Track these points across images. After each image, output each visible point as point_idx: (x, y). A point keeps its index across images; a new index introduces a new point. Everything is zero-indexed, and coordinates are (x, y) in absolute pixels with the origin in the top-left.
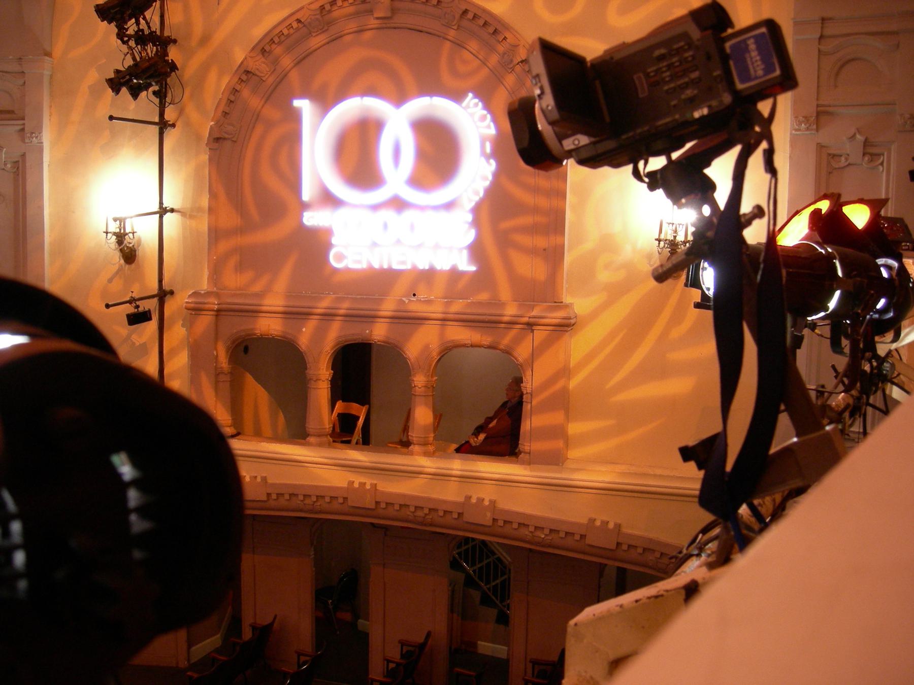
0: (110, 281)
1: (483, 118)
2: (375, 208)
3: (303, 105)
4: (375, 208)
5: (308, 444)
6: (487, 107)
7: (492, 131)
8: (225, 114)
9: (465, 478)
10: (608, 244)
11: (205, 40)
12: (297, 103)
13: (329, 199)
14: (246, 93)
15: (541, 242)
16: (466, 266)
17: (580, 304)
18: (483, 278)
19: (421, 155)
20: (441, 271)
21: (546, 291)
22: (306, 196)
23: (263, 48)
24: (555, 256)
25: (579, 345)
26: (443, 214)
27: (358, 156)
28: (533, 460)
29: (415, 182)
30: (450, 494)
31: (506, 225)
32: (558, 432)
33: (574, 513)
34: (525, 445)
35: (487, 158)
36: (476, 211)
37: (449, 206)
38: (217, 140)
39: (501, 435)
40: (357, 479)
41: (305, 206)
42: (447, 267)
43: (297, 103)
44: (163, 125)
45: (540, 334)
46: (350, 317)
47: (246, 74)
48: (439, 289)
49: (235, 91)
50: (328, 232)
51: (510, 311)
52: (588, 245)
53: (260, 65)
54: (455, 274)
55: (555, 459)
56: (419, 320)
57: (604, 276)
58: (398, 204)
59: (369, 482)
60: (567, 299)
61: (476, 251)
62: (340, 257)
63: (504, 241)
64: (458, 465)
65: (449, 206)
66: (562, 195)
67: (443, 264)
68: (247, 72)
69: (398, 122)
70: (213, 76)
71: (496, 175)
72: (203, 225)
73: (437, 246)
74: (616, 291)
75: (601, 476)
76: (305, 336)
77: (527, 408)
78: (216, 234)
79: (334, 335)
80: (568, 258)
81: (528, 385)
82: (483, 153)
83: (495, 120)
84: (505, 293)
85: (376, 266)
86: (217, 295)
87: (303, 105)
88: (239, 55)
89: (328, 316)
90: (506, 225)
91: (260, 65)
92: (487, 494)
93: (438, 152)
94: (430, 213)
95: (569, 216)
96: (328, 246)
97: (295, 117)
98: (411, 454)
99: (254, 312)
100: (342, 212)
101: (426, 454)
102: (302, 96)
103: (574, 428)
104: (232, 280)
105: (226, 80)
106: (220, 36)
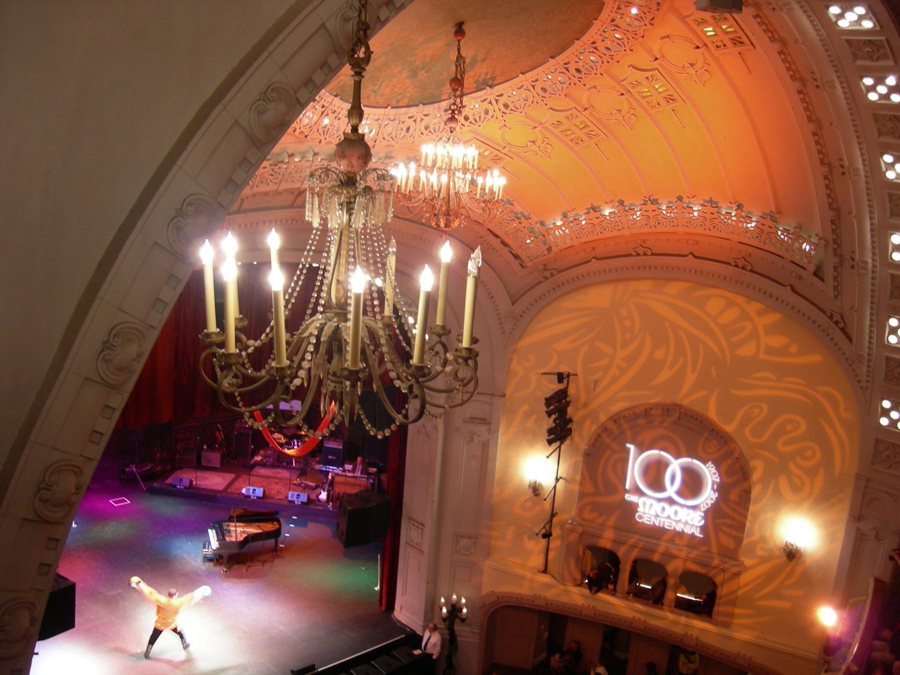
0: (525, 501)
1: (715, 474)
2: (660, 500)
3: (632, 447)
4: (660, 500)
5: (617, 597)
6: (717, 469)
7: (718, 480)
8: (593, 445)
9: (686, 625)
10: (763, 540)
11: (585, 405)
12: (628, 445)
13: (638, 492)
14: (604, 436)
15: (734, 533)
16: (698, 534)
17: (748, 562)
18: (705, 541)
19: (684, 482)
20: (687, 534)
21: (731, 554)
22: (627, 487)
23: (616, 419)
24: (739, 541)
25: (744, 578)
26: (691, 511)
27: (654, 476)
28: (716, 624)
29: (680, 493)
30: (679, 630)
31: (718, 521)
32: (732, 615)
33: (732, 648)
34: (714, 616)
35: (714, 491)
36: (706, 512)
37: (694, 508)
38: (587, 455)
39: (704, 608)
40: (637, 616)
41: (627, 491)
42: (690, 533)
43: (628, 445)
45: (727, 575)
46: (643, 549)
47: (604, 429)
48: (685, 541)
49: (599, 435)
50: (637, 505)
51: (716, 562)
52: (754, 538)
53: (612, 426)
54: (693, 536)
55: (727, 625)
56: (675, 557)
57: (759, 552)
58: (671, 501)
59: (642, 618)
60: (742, 559)
61: (703, 529)
62: (640, 517)
63: (717, 528)
64: (683, 619)
65: (694, 508)
66: (746, 517)
67: (688, 530)
68: (606, 429)
69: (675, 466)
70: (588, 423)
71: (717, 499)
72: (576, 487)
73: (686, 523)
74: (763, 560)
75: (744, 635)
76: (621, 552)
77: (717, 601)
78: (582, 495)
79: (634, 554)
80: (745, 542)
81: (721, 592)
82: (713, 488)
83: (720, 475)
84: (715, 549)
85: (657, 524)
86: (582, 526)
87: (632, 447)
88: (603, 418)
89: (634, 546)
90: (718, 521)
91: (612, 426)
92: (695, 633)
93: (692, 484)
94: (686, 510)
95: (748, 524)
96: (637, 511)
97: (627, 451)
98: (661, 609)
99: (600, 537)
100: (643, 499)
101: (671, 612)
102: (631, 443)
103: (737, 611)
104: (587, 515)
105: (594, 428)
106: (594, 404)
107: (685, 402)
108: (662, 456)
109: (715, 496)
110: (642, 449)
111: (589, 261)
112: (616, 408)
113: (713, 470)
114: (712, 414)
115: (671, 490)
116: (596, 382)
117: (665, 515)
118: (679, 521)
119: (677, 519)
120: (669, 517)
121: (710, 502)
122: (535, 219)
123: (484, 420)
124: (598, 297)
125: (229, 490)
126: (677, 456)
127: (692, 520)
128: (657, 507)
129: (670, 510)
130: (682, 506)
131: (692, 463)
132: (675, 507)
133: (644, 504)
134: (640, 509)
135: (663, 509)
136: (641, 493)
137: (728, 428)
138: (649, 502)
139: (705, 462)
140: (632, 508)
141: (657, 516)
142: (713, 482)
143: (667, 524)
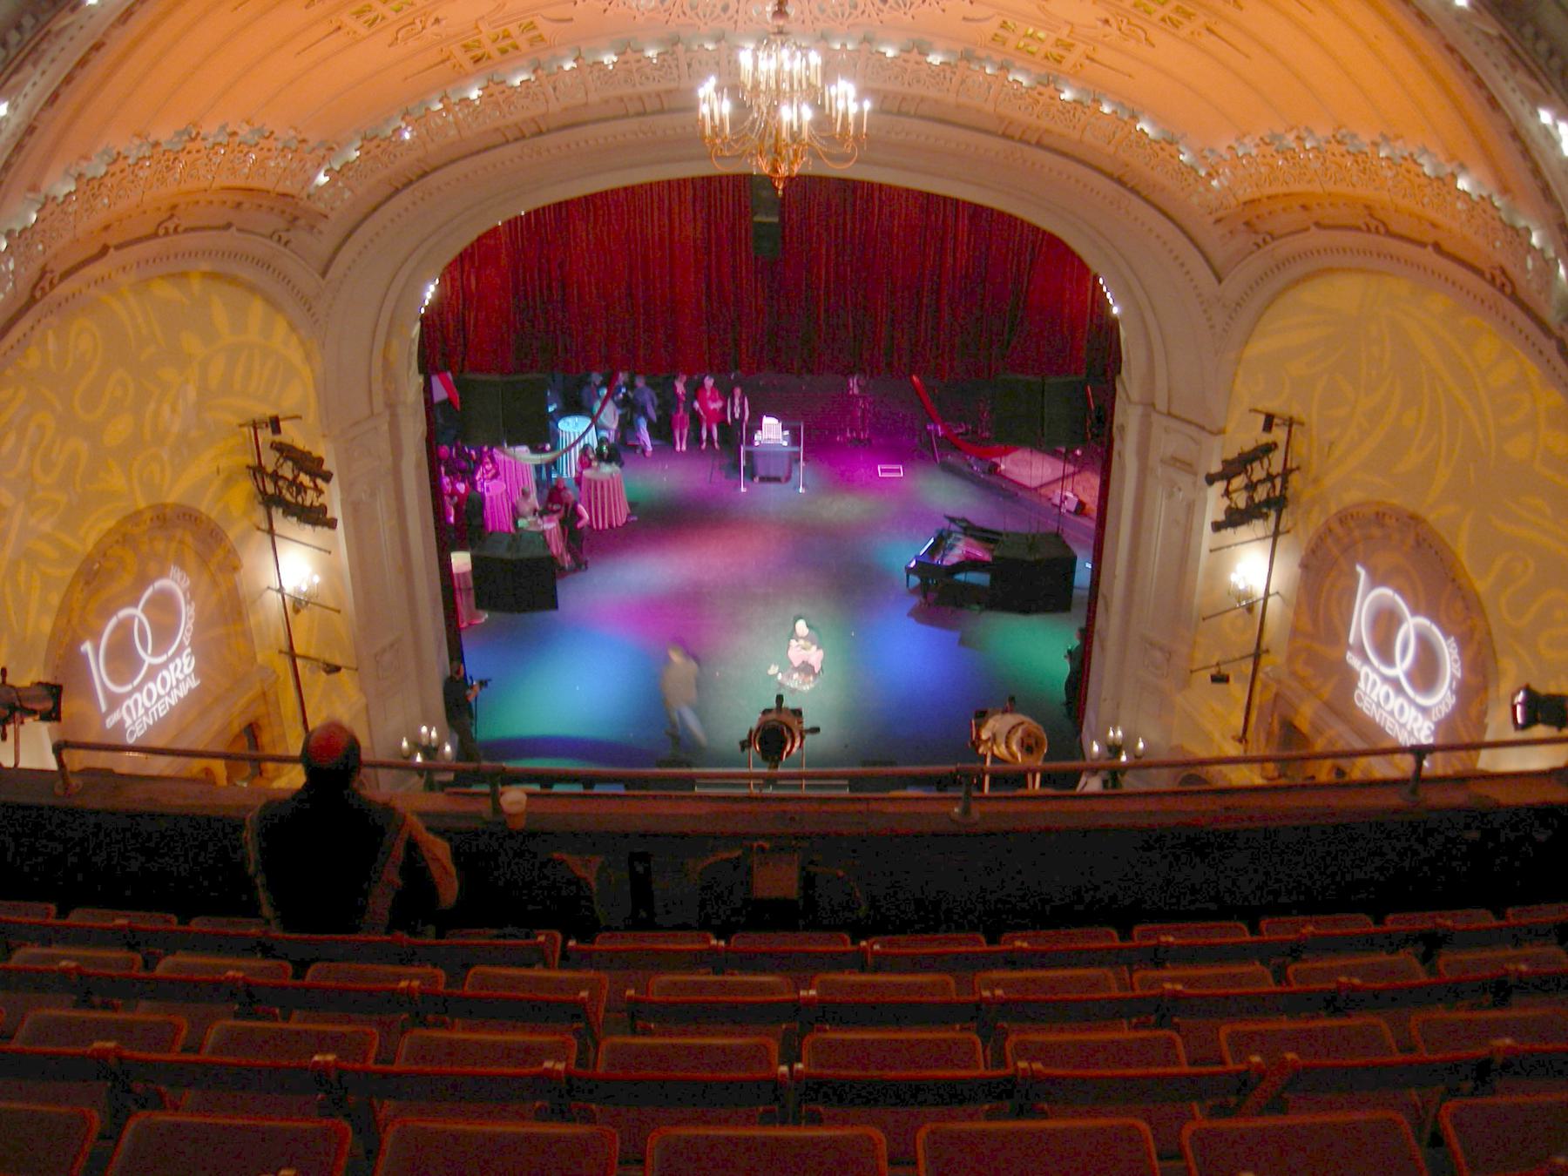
2: (1386, 679)
6: (1461, 654)
7: (1459, 675)
8: (1313, 552)
14: (1329, 541)
19: (1418, 660)
29: (1410, 676)
37: (1425, 710)
44: (1276, 535)
53: (1336, 527)
65: (1425, 710)
69: (1412, 625)
73: (1411, 733)
83: (1462, 666)
97: (1356, 577)
102: (1364, 565)
107: (1431, 517)
108: (1395, 603)
109: (1452, 701)
110: (1375, 581)
111: (1307, 229)
112: (1352, 496)
113: (1455, 652)
114: (1462, 549)
115: (1400, 669)
116: (1331, 444)
117: (1388, 708)
118: (1403, 726)
119: (1403, 720)
120: (1391, 713)
121: (1445, 710)
122: (1324, 132)
123: (1190, 465)
124: (1343, 293)
125: (1043, 491)
126: (1415, 612)
127: (1420, 730)
128: (1383, 689)
129: (1395, 702)
130: (1412, 702)
131: (1429, 629)
132: (1401, 700)
133: (1367, 676)
134: (1361, 684)
135: (1387, 697)
136: (1366, 660)
137: (1482, 586)
138: (1373, 676)
139: (1446, 635)
140: (1349, 680)
141: (1378, 705)
142: (1453, 676)
143: (1391, 727)
